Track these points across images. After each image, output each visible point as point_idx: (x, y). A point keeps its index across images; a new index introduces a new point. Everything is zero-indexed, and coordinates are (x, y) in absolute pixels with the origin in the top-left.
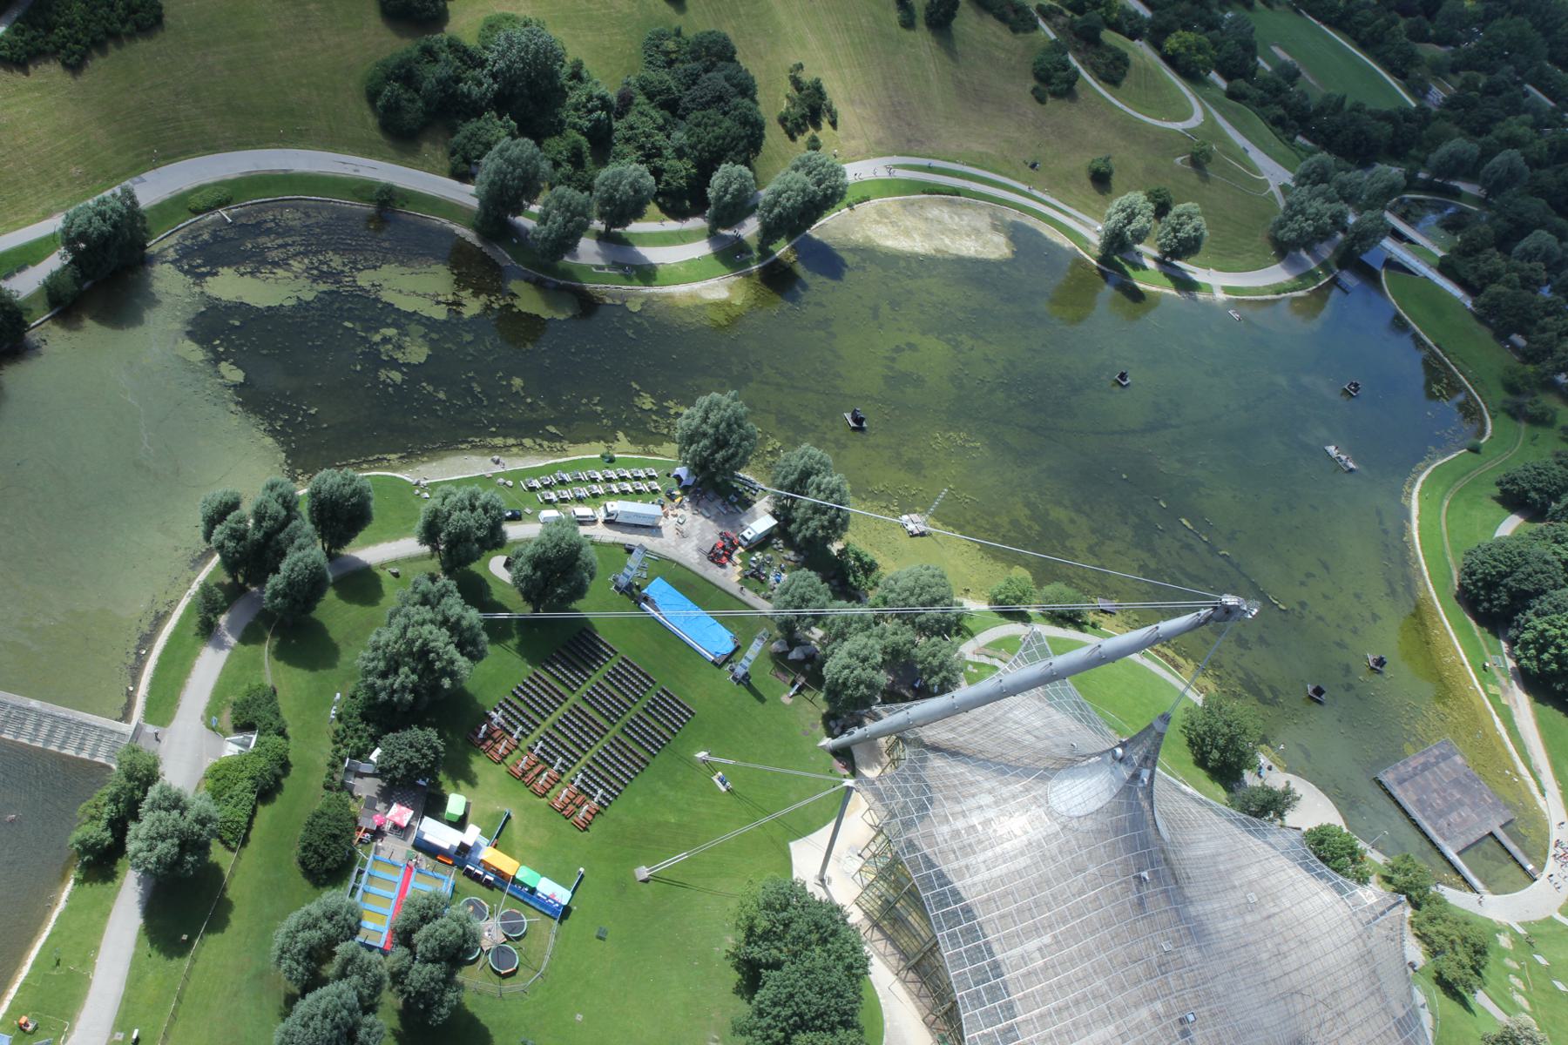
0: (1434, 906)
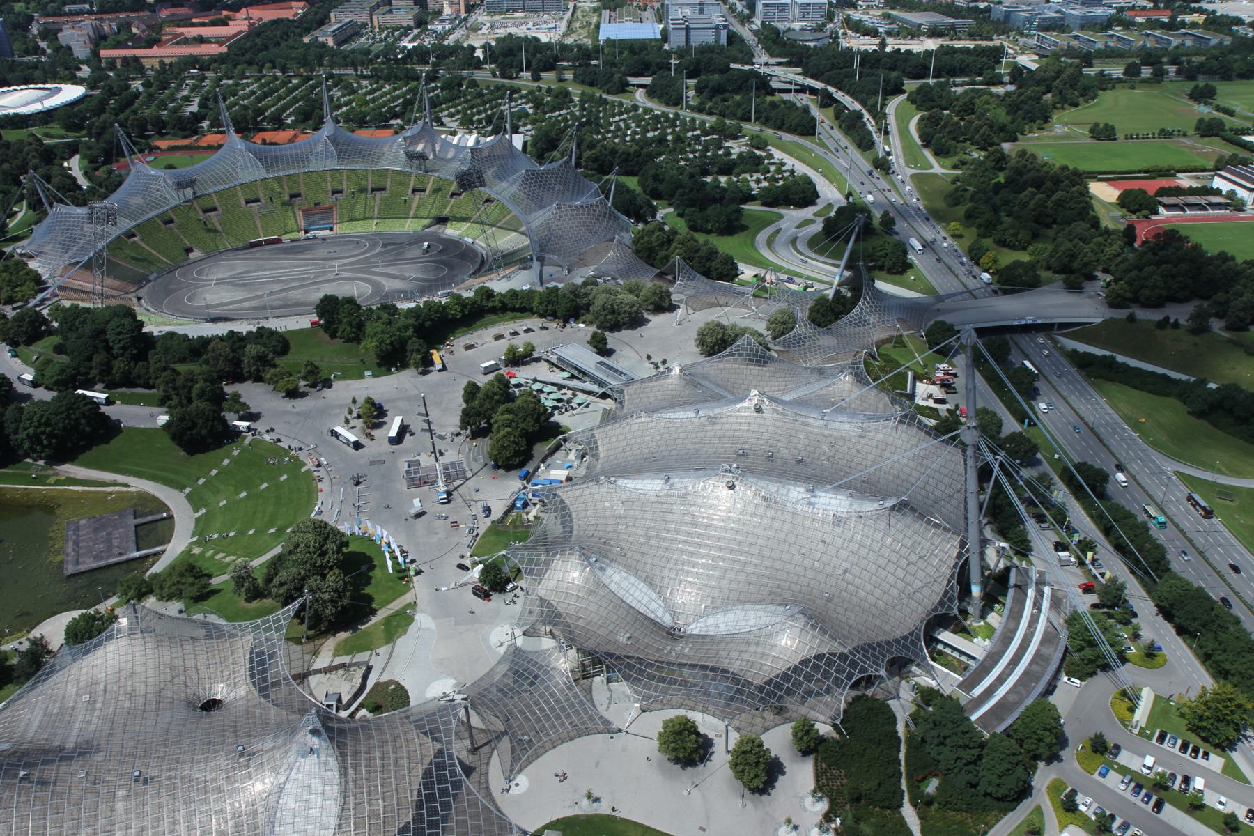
0: (154, 582)
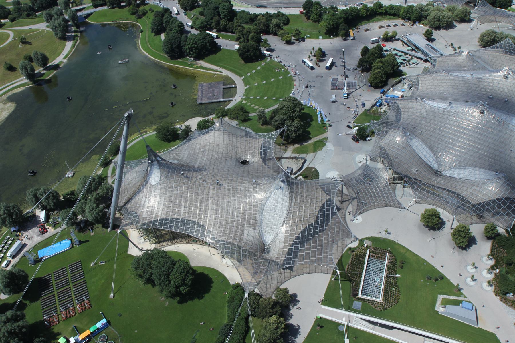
0: (229, 112)
